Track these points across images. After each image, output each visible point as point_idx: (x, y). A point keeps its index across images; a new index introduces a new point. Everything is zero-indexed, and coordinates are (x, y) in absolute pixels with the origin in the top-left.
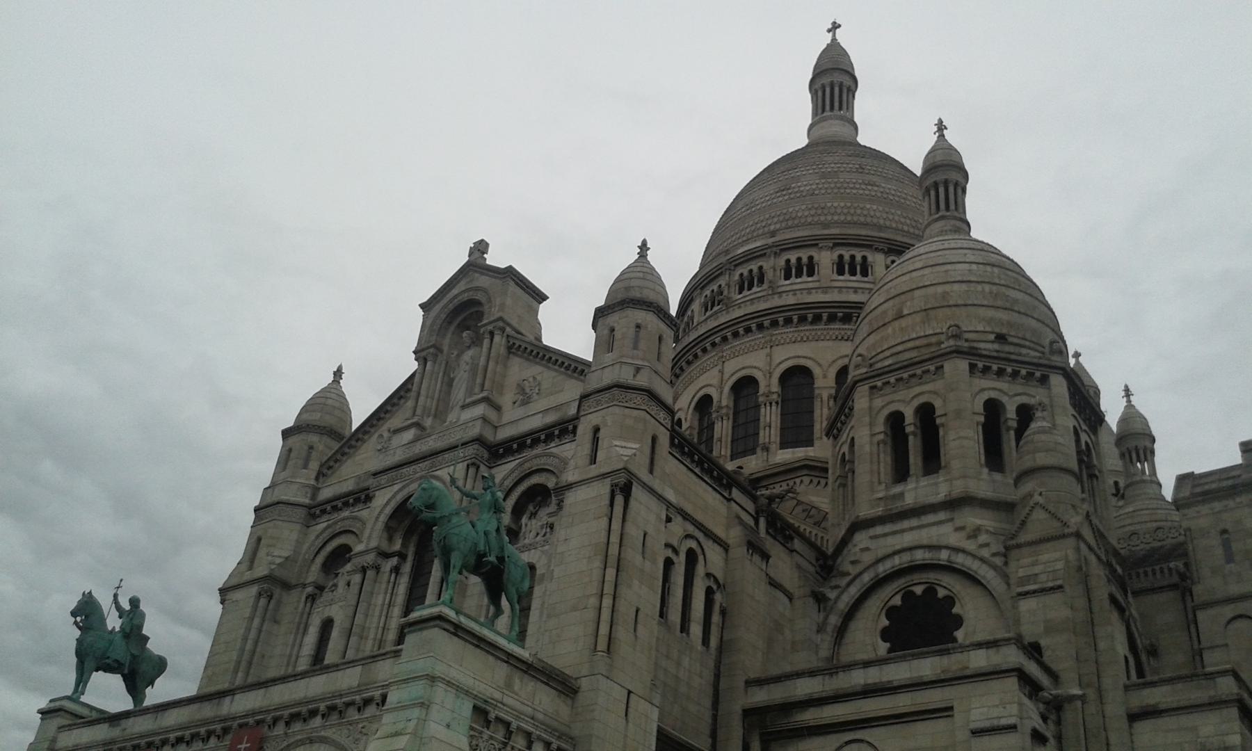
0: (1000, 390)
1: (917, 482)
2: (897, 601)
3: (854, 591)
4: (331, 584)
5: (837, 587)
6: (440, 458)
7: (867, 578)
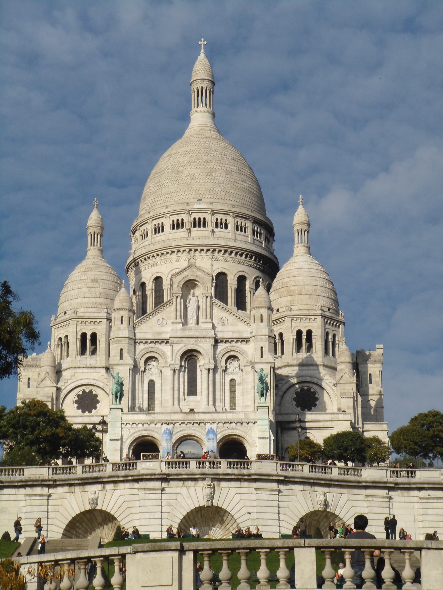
5: (281, 383)
6: (199, 339)
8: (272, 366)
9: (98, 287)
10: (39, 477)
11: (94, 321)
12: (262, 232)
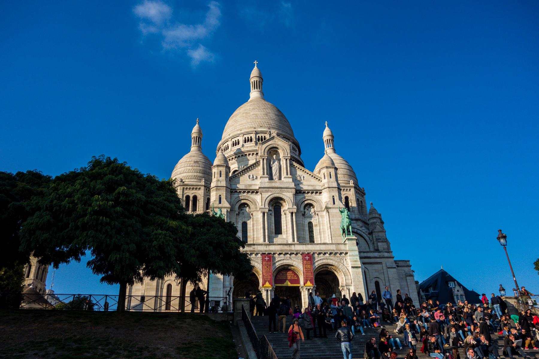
0: (358, 196)
4: (241, 212)
9: (199, 166)
11: (195, 188)
12: (297, 149)
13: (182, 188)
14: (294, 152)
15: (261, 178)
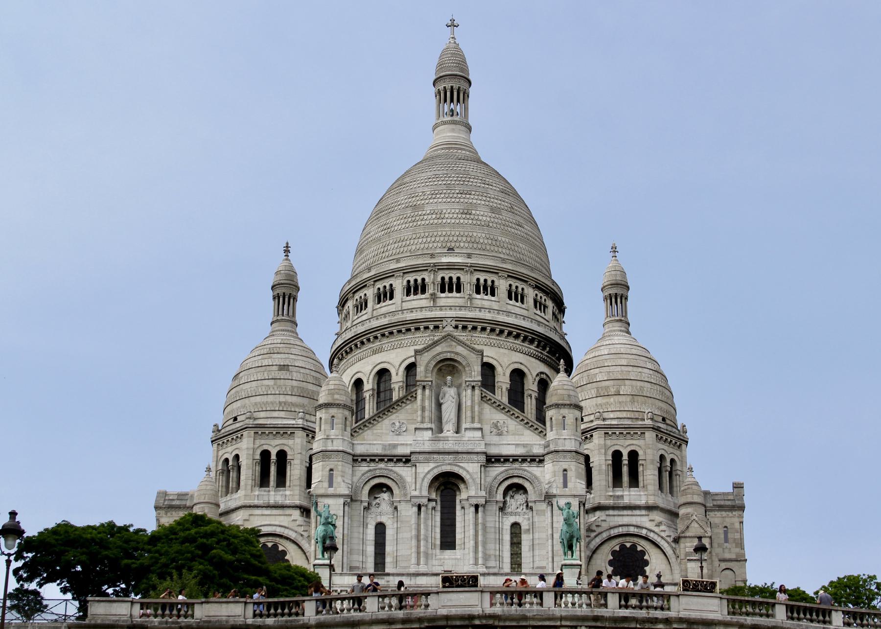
0: (665, 450)
1: (629, 491)
2: (617, 548)
3: (598, 540)
7: (605, 535)
8: (581, 502)
9: (290, 378)
10: (227, 622)
11: (282, 432)
12: (550, 304)
13: (252, 432)
14: (538, 312)
15: (417, 432)
